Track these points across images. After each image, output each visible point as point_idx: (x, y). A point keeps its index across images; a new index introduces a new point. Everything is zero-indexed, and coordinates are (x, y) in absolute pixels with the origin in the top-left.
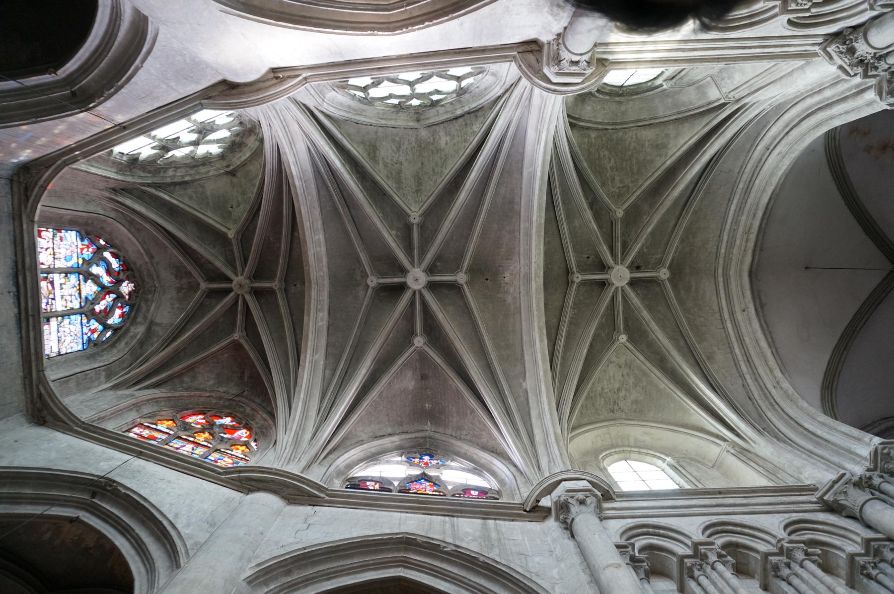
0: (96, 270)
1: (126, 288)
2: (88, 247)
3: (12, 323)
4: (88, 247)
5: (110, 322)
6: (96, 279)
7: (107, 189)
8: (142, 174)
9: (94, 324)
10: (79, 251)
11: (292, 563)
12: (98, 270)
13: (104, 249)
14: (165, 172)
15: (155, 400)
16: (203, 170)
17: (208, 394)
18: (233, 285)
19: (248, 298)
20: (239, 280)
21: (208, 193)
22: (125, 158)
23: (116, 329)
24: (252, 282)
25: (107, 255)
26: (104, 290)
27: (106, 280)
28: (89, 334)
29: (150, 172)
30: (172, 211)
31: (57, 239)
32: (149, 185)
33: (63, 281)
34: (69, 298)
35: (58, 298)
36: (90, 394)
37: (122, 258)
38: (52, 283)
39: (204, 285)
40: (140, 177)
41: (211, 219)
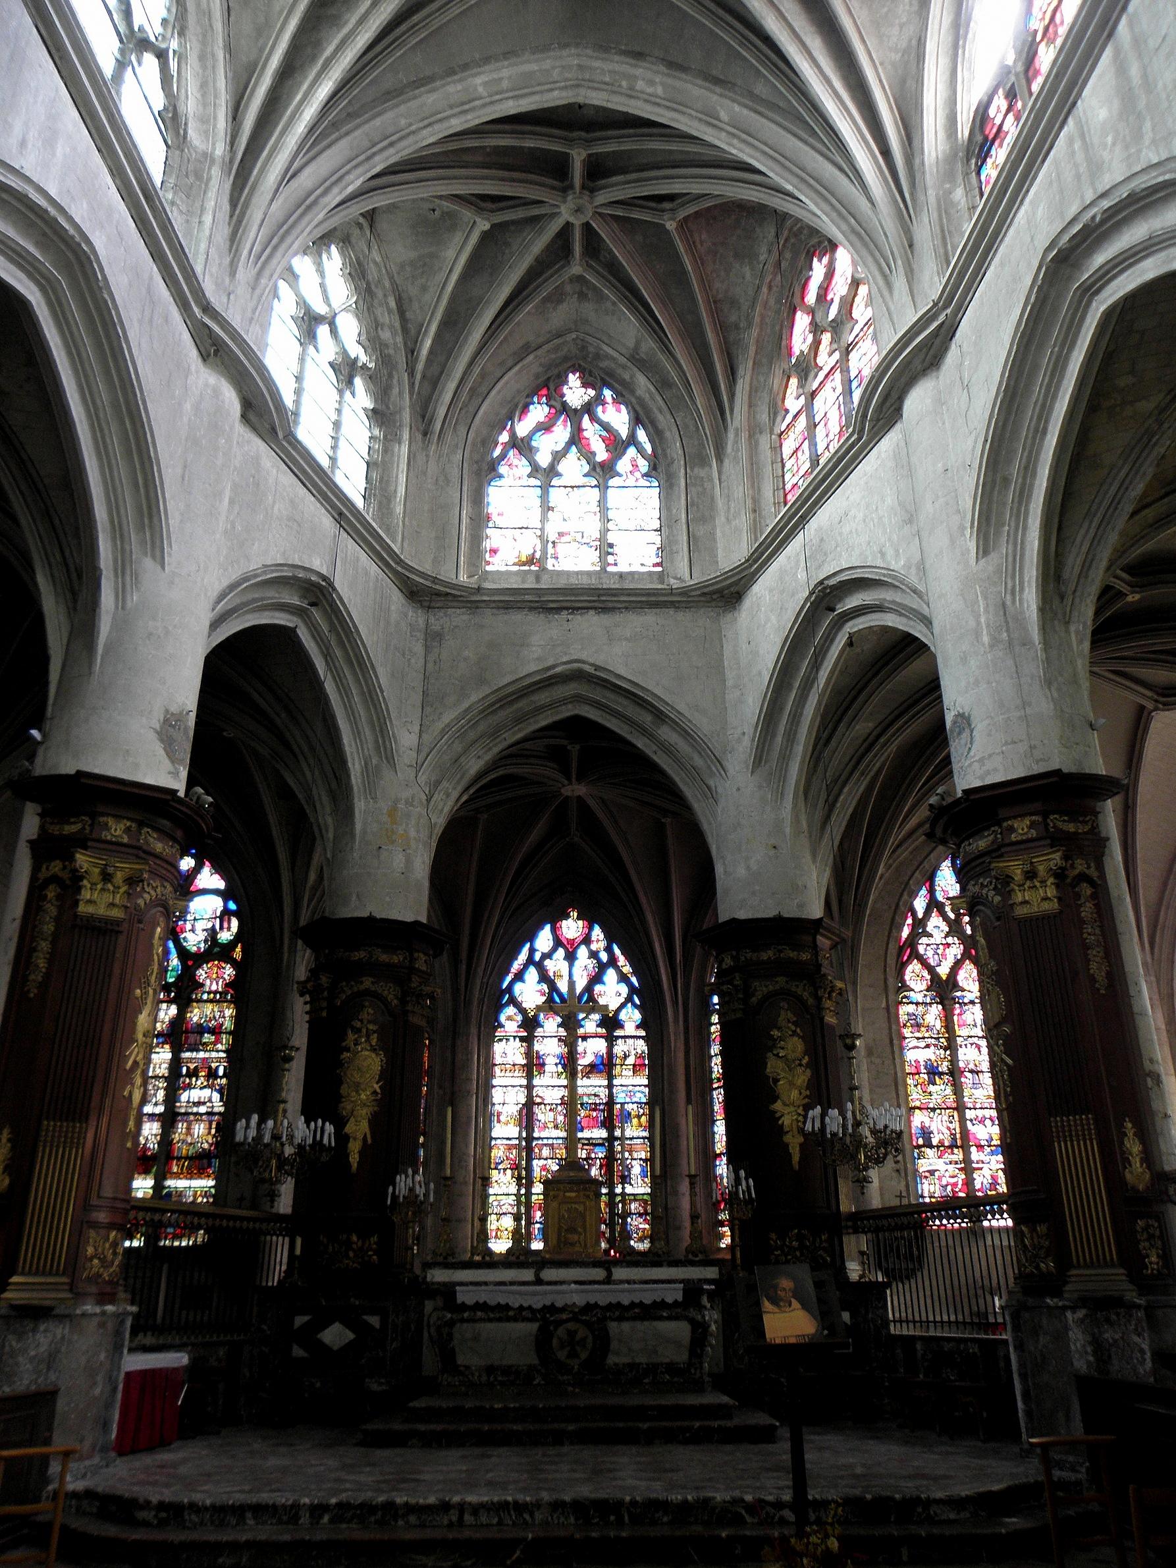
1: (575, 393)
3: (606, 620)
5: (624, 433)
6: (558, 456)
7: (426, 448)
8: (396, 391)
9: (623, 465)
11: (995, 471)
14: (387, 346)
15: (753, 391)
16: (372, 273)
17: (765, 290)
18: (577, 222)
19: (602, 198)
20: (567, 211)
21: (413, 255)
22: (376, 432)
23: (636, 420)
24: (571, 187)
26: (576, 439)
28: (638, 475)
29: (390, 376)
30: (454, 323)
31: (500, 523)
32: (412, 374)
36: (720, 503)
37: (528, 400)
38: (561, 534)
39: (576, 269)
40: (401, 393)
41: (456, 254)
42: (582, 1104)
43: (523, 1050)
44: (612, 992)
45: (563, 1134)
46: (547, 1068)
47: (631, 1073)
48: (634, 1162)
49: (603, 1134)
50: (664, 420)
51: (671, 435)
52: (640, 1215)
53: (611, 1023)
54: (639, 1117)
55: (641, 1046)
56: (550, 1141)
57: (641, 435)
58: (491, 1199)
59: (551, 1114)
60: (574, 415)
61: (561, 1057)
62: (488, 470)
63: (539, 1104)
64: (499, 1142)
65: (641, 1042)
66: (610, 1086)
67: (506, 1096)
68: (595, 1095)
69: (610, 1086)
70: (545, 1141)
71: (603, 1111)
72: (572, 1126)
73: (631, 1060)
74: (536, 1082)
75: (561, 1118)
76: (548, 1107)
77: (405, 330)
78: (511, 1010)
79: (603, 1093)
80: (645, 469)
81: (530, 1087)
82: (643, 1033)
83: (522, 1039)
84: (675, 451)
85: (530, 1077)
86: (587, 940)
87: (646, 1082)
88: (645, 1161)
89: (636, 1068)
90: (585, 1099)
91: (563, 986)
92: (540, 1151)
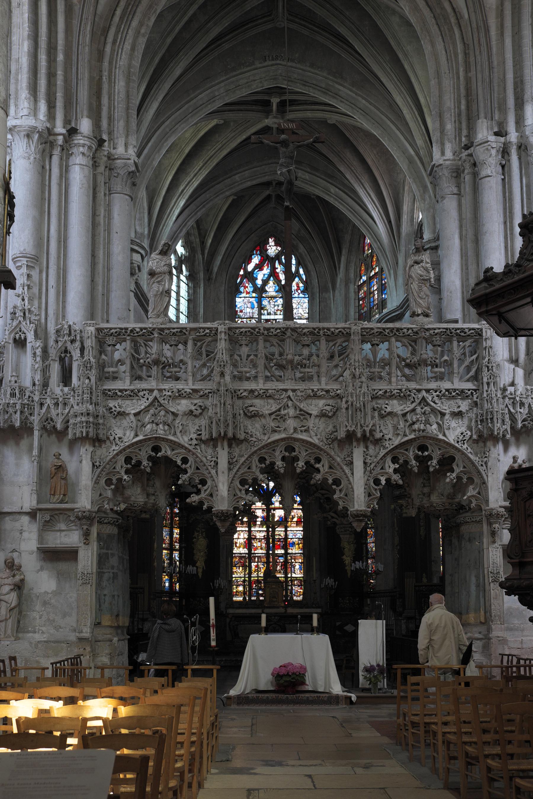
0: (259, 282)
1: (272, 250)
2: (245, 287)
4: (245, 287)
6: (265, 282)
8: (197, 263)
10: (248, 295)
12: (260, 276)
13: (245, 270)
14: (192, 243)
22: (190, 285)
25: (250, 267)
26: (273, 274)
27: (266, 271)
28: (299, 291)
32: (203, 254)
33: (266, 312)
34: (276, 308)
35: (276, 317)
36: (333, 311)
45: (264, 552)
49: (283, 551)
50: (311, 267)
51: (313, 274)
52: (299, 586)
54: (298, 544)
55: (300, 513)
57: (301, 271)
58: (234, 579)
60: (271, 261)
62: (236, 291)
65: (300, 511)
66: (286, 531)
69: (286, 531)
73: (295, 519)
74: (252, 529)
75: (264, 545)
77: (200, 234)
79: (283, 534)
80: (302, 289)
81: (250, 531)
82: (301, 507)
84: (315, 282)
85: (250, 527)
87: (302, 529)
88: (301, 563)
89: (298, 523)
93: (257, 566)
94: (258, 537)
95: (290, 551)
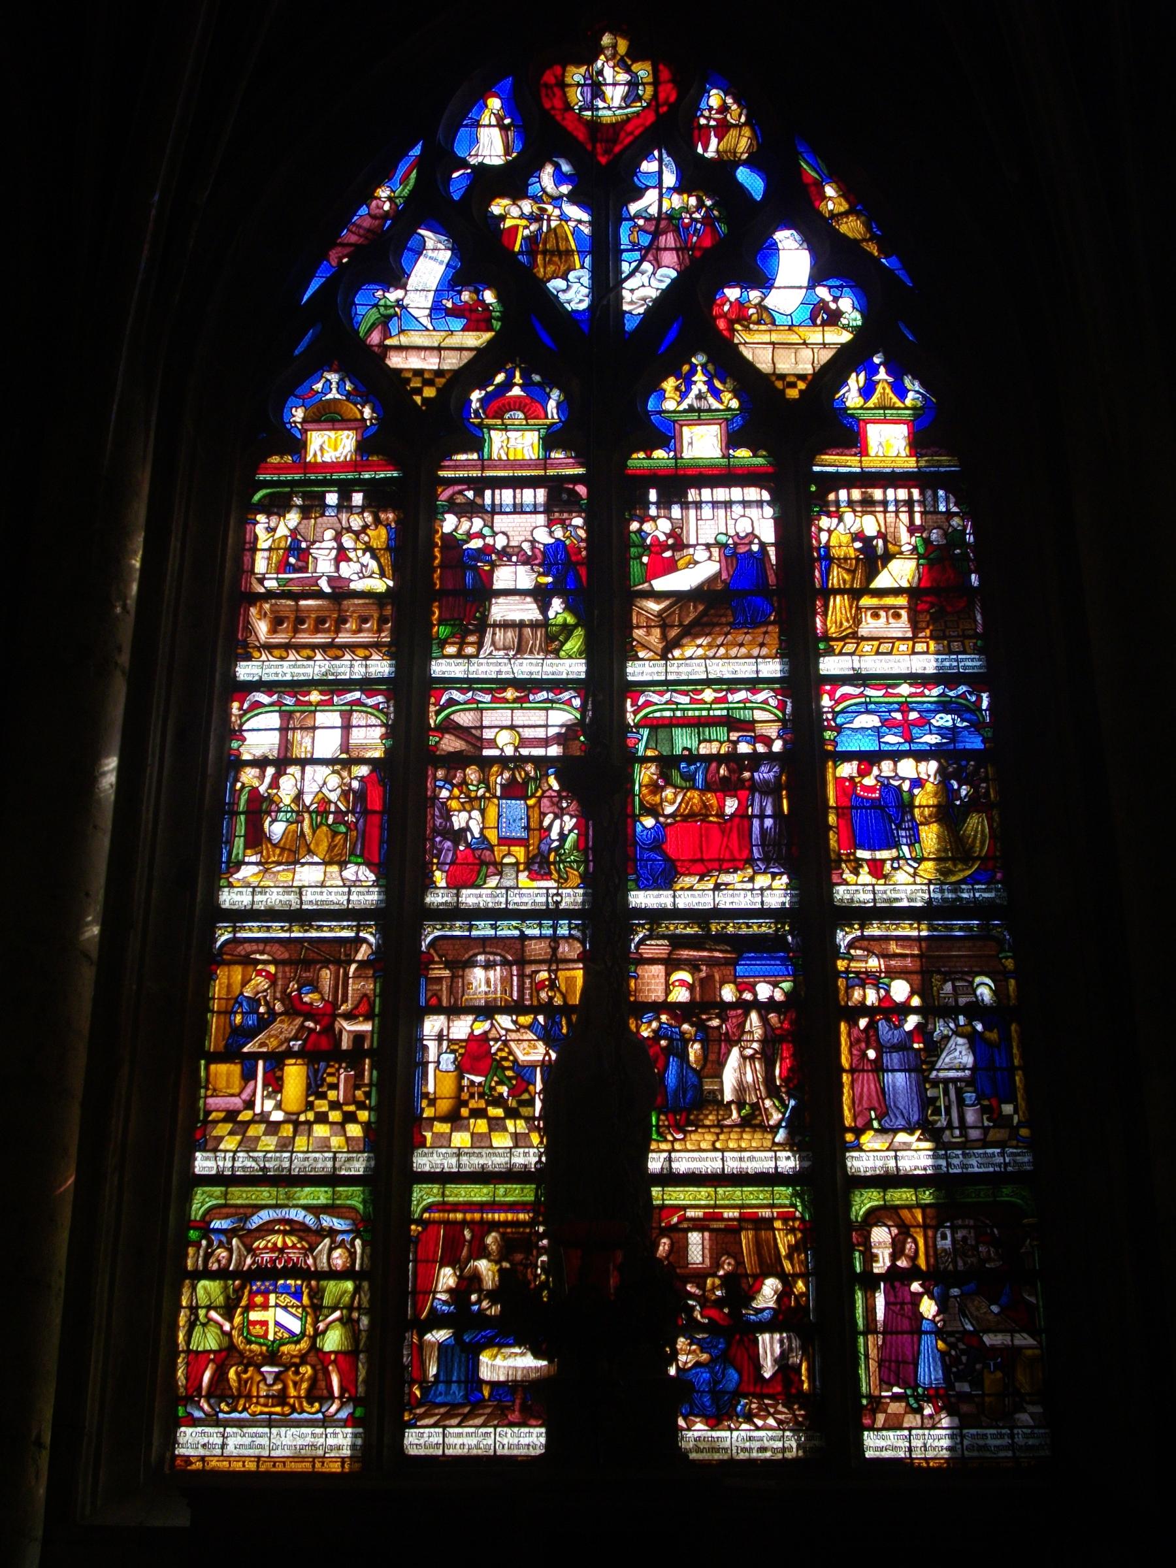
42: (667, 763)
43: (379, 537)
44: (793, 312)
46: (500, 610)
47: (901, 627)
48: (941, 1028)
53: (791, 434)
56: (508, 929)
59: (516, 808)
61: (552, 559)
63: (457, 761)
64: (252, 931)
67: (303, 737)
68: (731, 723)
70: (483, 929)
71: (771, 790)
72: (615, 856)
75: (563, 826)
76: (499, 779)
78: (331, 386)
83: (378, 497)
86: (671, 127)
90: (683, 740)
91: (574, 292)
92: (460, 966)
93: (475, 1055)
94: (505, 743)
95: (856, 888)
